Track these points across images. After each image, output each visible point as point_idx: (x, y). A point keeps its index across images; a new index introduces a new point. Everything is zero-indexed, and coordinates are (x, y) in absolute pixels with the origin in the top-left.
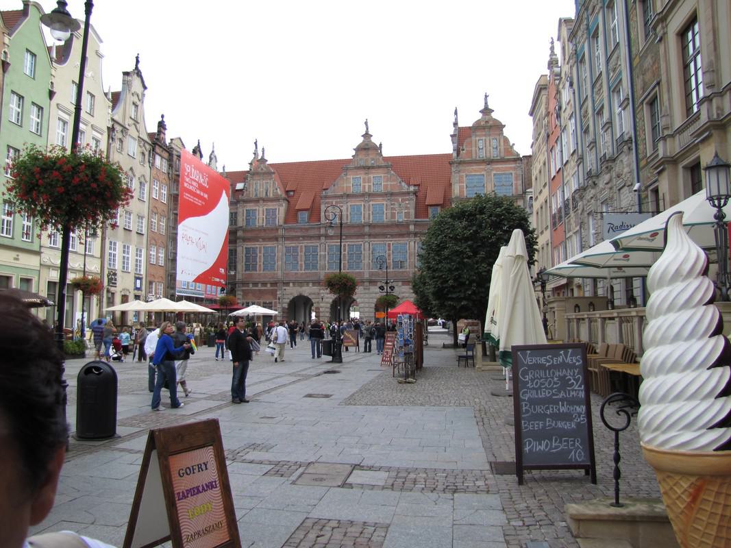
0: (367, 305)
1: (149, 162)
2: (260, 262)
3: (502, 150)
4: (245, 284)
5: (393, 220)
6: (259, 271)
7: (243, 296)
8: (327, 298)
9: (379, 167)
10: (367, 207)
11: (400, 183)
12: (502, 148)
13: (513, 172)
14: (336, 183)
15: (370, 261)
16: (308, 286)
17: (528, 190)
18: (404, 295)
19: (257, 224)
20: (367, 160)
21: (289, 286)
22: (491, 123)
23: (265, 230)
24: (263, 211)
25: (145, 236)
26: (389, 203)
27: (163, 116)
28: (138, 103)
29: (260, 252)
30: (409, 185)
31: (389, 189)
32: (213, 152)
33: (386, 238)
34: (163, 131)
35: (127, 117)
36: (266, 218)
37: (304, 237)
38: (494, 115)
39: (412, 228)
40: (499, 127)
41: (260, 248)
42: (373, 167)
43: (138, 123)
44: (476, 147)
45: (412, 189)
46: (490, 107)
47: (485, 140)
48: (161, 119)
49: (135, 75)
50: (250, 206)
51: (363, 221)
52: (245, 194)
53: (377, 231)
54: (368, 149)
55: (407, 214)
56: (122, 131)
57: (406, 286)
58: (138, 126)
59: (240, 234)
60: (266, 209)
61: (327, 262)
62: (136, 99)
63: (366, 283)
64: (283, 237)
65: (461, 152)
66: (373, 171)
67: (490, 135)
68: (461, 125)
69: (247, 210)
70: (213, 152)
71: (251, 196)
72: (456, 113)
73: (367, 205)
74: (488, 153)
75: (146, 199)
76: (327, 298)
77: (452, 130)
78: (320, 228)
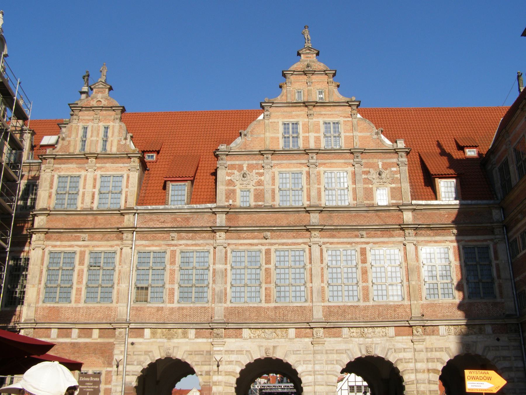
2: (80, 282)
5: (368, 202)
6: (78, 301)
8: (230, 362)
10: (312, 176)
14: (249, 129)
15: (325, 285)
16: (185, 335)
20: (309, 92)
21: (142, 336)
24: (95, 179)
26: (359, 169)
29: (81, 263)
31: (357, 144)
41: (82, 253)
42: (322, 104)
57: (404, 337)
63: (315, 330)
64: (133, 229)
71: (71, 150)
73: (314, 171)
76: (230, 362)
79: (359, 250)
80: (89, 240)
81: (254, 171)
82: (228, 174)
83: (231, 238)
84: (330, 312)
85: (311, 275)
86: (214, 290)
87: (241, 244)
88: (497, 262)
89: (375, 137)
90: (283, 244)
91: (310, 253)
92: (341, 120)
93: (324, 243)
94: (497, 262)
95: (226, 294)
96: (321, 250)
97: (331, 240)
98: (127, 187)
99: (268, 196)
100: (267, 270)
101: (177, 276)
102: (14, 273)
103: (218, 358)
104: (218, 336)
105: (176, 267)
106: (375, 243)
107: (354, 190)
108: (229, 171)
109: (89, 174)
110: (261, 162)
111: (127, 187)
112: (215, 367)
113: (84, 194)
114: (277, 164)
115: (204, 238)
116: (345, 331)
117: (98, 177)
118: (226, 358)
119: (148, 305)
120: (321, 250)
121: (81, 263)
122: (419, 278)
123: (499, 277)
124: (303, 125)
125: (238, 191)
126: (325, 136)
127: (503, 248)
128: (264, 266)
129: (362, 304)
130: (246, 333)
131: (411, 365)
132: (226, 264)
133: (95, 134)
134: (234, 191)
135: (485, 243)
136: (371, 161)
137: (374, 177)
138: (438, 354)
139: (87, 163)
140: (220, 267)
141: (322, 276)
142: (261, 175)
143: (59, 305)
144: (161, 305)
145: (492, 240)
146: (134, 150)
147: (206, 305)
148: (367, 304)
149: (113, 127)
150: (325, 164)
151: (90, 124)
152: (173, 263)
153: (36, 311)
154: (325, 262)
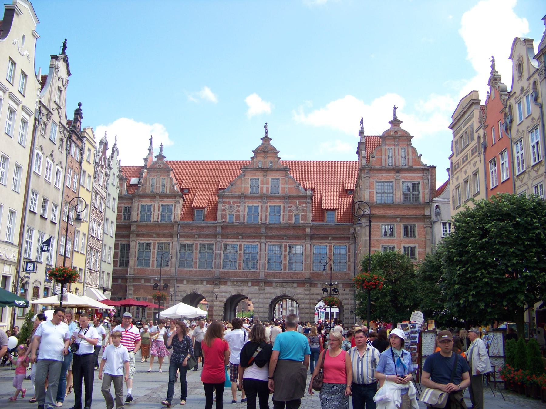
0: (261, 305)
1: (66, 149)
2: (153, 257)
3: (411, 160)
4: (136, 279)
5: (290, 222)
6: (153, 266)
7: (134, 291)
8: (222, 297)
9: (278, 170)
10: (264, 208)
11: (297, 186)
12: (410, 157)
13: (421, 181)
15: (266, 262)
16: (202, 283)
17: (434, 199)
18: (299, 296)
19: (152, 220)
21: (182, 283)
22: (399, 133)
23: (160, 226)
24: (159, 207)
25: (58, 225)
26: (286, 206)
27: (80, 105)
28: (63, 88)
30: (306, 190)
32: (115, 144)
33: (283, 239)
34: (79, 119)
35: (52, 102)
36: (161, 214)
37: (200, 236)
38: (402, 126)
39: (308, 230)
40: (408, 138)
41: (154, 244)
42: (271, 170)
43: (61, 108)
44: (385, 155)
45: (309, 193)
46: (398, 118)
47: (394, 149)
48: (78, 107)
49: (62, 60)
50: (146, 202)
51: (260, 221)
52: (141, 188)
53: (273, 232)
54: (268, 152)
55: (304, 217)
56: (47, 115)
57: (301, 288)
58: (60, 111)
59: (133, 228)
60: (162, 205)
61: (222, 261)
62: (60, 84)
65: (371, 159)
66: (272, 173)
67: (398, 145)
68: (365, 134)
69: (142, 205)
70: (115, 144)
71: (147, 192)
72: (362, 122)
73: (264, 206)
74: (397, 161)
75: (60, 187)
76: (222, 297)
77: (358, 139)
78: (216, 227)
79: (283, 246)
80: (157, 237)
81: (236, 205)
82: (223, 206)
83: (223, 238)
84: (268, 275)
85: (260, 257)
86: (215, 262)
87: (228, 241)
88: (350, 254)
89: (296, 188)
90: (248, 242)
91: (260, 247)
92: (280, 178)
93: (267, 242)
94: (350, 254)
95: (220, 265)
96: (266, 245)
97: (271, 241)
98: (175, 211)
99: (242, 218)
100: (240, 254)
101: (198, 255)
102: (122, 251)
103: (216, 294)
104: (216, 284)
105: (198, 251)
106: (291, 242)
107: (283, 215)
108: (224, 204)
109: (156, 204)
110: (239, 200)
111: (175, 211)
112: (215, 298)
113: (154, 214)
114: (247, 201)
115: (211, 238)
116: (274, 284)
117: (161, 205)
118: (220, 294)
119: (185, 269)
120: (266, 245)
121: (154, 248)
122: (310, 260)
123: (349, 261)
124: (261, 180)
125: (227, 215)
126: (271, 186)
127: (352, 247)
128: (239, 252)
129: (283, 271)
130: (229, 283)
131: (303, 300)
132: (221, 251)
133: (158, 183)
134: (226, 215)
135: (345, 244)
136: (293, 201)
137: (294, 209)
138: (316, 296)
139: (155, 198)
140: (218, 252)
141: (265, 257)
142: (239, 206)
143: (144, 268)
144: (191, 269)
145: (348, 243)
146: (178, 192)
147: (212, 270)
148: (285, 271)
149: (167, 179)
150: (270, 202)
151: (156, 177)
152: (196, 249)
153: (134, 270)
154: (267, 251)
